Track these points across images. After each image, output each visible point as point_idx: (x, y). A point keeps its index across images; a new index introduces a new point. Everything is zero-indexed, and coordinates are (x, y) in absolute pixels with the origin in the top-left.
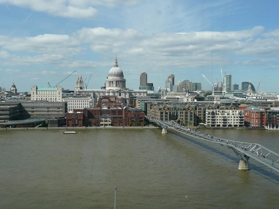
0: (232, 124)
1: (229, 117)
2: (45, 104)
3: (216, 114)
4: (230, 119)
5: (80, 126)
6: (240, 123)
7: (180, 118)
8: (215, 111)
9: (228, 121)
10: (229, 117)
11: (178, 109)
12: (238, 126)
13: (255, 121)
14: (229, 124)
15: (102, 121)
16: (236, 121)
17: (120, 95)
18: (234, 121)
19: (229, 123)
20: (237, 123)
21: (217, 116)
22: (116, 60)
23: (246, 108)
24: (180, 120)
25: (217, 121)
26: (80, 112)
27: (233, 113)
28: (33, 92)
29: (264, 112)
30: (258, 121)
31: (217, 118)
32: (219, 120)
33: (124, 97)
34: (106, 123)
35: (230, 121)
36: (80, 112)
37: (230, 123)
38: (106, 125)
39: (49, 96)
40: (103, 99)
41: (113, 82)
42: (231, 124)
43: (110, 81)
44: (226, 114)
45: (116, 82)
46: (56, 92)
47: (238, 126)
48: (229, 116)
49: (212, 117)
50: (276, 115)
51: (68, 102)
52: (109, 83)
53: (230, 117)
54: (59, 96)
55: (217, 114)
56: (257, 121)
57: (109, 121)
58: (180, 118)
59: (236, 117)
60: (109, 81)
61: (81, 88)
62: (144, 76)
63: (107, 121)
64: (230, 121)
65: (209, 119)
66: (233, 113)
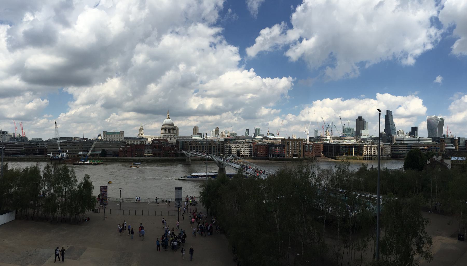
0: (244, 155)
3: (232, 147)
4: (243, 151)
6: (250, 154)
7: (206, 151)
8: (231, 145)
9: (241, 153)
11: (205, 144)
12: (249, 156)
14: (242, 155)
15: (146, 153)
16: (247, 153)
18: (245, 153)
19: (242, 154)
20: (248, 154)
21: (233, 148)
24: (205, 152)
25: (233, 153)
26: (129, 146)
29: (267, 146)
31: (233, 151)
32: (234, 152)
34: (148, 155)
36: (129, 146)
37: (243, 154)
38: (149, 156)
39: (118, 138)
40: (155, 140)
41: (165, 130)
45: (168, 130)
47: (249, 156)
48: (241, 148)
49: (229, 150)
50: (274, 147)
51: (128, 142)
53: (243, 149)
54: (122, 138)
57: (151, 153)
59: (247, 149)
63: (149, 153)
64: (243, 153)
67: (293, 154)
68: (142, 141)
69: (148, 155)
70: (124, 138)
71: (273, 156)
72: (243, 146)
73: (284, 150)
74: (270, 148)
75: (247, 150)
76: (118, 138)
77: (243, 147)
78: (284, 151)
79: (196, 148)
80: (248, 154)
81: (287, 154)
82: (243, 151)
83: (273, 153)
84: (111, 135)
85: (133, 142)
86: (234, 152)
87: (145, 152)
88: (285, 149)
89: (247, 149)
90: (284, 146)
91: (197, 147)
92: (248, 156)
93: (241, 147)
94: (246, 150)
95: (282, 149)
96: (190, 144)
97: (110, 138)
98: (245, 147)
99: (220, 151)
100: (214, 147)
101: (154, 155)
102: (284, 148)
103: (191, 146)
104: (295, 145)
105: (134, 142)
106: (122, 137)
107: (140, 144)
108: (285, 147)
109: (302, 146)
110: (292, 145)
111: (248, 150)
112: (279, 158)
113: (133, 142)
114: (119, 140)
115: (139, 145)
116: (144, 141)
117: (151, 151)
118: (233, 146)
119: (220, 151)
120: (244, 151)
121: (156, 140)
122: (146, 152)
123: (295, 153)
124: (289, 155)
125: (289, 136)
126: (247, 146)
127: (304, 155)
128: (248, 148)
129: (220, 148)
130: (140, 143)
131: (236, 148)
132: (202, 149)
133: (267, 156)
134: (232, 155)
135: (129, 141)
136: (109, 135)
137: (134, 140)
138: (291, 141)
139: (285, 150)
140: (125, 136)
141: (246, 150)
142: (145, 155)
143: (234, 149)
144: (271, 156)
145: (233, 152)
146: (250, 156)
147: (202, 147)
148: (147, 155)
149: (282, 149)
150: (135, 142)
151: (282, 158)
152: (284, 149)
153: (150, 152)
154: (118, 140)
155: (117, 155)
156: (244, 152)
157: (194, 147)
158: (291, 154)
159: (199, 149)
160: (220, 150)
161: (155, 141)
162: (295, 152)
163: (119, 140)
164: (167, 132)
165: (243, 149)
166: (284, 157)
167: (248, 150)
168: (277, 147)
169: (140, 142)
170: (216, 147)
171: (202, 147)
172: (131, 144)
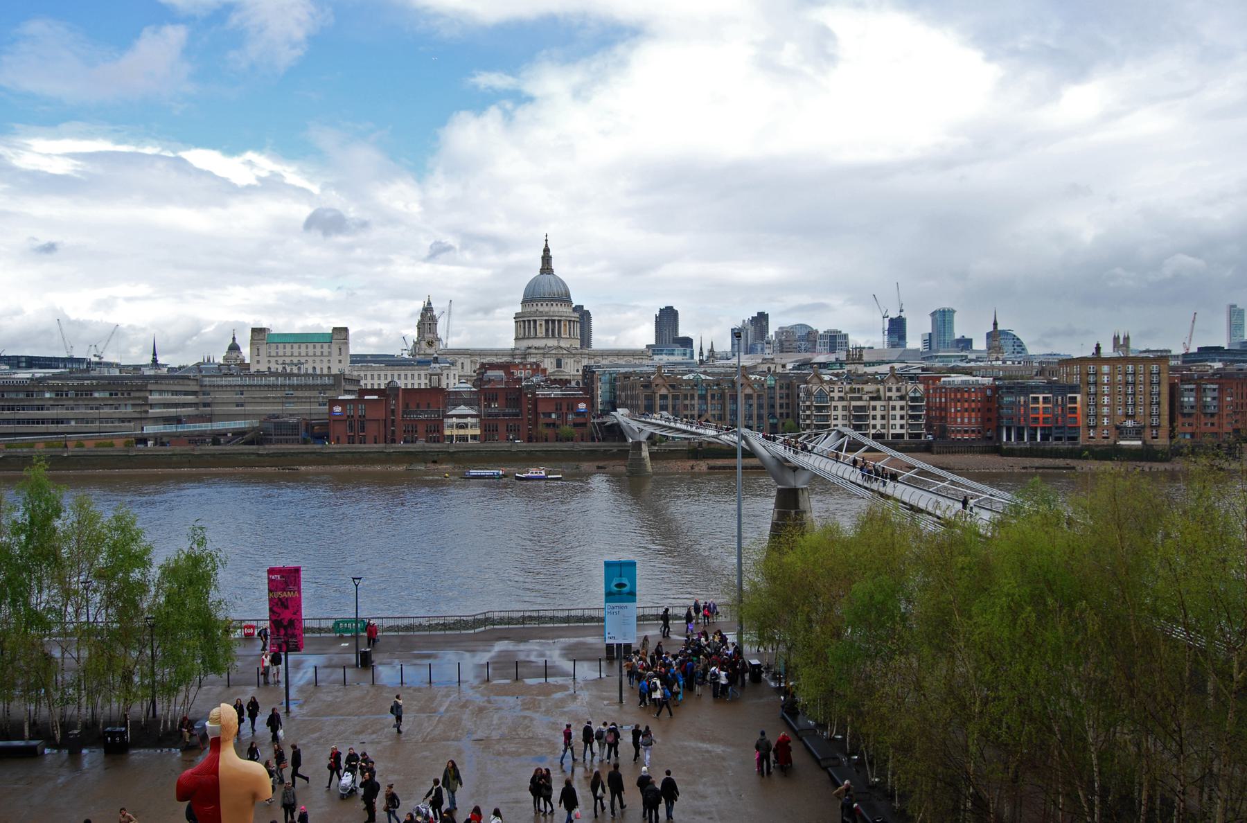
1: (874, 408)
2: (277, 379)
5: (375, 443)
8: (827, 388)
9: (873, 422)
10: (874, 408)
12: (906, 438)
13: (959, 420)
14: (873, 431)
15: (451, 426)
16: (898, 422)
17: (559, 365)
19: (874, 426)
21: (834, 404)
22: (547, 250)
23: (939, 381)
26: (376, 397)
27: (889, 394)
28: (258, 349)
30: (970, 419)
32: (840, 417)
33: (572, 373)
34: (462, 432)
35: (878, 422)
36: (376, 397)
38: (463, 438)
40: (489, 369)
41: (535, 321)
42: (882, 431)
43: (525, 319)
44: (866, 397)
45: (547, 321)
46: (329, 347)
47: (906, 438)
48: (873, 403)
49: (819, 409)
51: (369, 377)
52: (524, 328)
54: (340, 361)
55: (836, 398)
56: (966, 420)
58: (714, 416)
59: (898, 408)
60: (524, 321)
61: (430, 344)
62: (667, 318)
65: (808, 417)
66: (889, 394)
67: (1117, 428)
68: (431, 375)
69: (462, 432)
70: (352, 362)
71: (1020, 437)
72: (878, 391)
73: (1075, 408)
74: (1007, 399)
75: (898, 413)
76: (325, 359)
77: (878, 398)
78: (1074, 413)
79: (670, 402)
80: (902, 427)
81: (1089, 427)
82: (878, 413)
83: (1022, 423)
84: (288, 346)
85: (393, 375)
86: (840, 417)
87: (445, 420)
88: (1078, 405)
89: (899, 404)
90: (1074, 389)
91: (675, 398)
92: (901, 436)
93: (872, 399)
94: (894, 408)
95: (1064, 404)
96: (647, 386)
97: (288, 360)
98: (890, 398)
99: (778, 416)
100: (748, 397)
101: (489, 430)
102: (1075, 398)
103: (648, 392)
104: (1127, 383)
105: (396, 379)
106: (340, 358)
107: (423, 387)
108: (1079, 397)
109: (1165, 390)
110: (1111, 384)
111: (902, 408)
112: (1052, 443)
113: (393, 375)
114: (329, 368)
115: (419, 390)
116: (439, 371)
117: (472, 416)
118: (836, 395)
119: (778, 416)
120: (883, 413)
121: (493, 366)
122: (450, 421)
123: (1129, 423)
124: (1099, 430)
125: (1098, 345)
126: (898, 394)
127: (1172, 437)
128: (903, 403)
129: (778, 401)
130: (423, 383)
131: (845, 403)
132: (696, 409)
133: (990, 438)
134: (839, 432)
135: (372, 375)
136: (281, 346)
137: (396, 368)
138: (1106, 369)
139: (1079, 411)
140: (352, 352)
141: (894, 408)
142: (447, 432)
143: (840, 404)
144: (1009, 438)
145: (837, 419)
146: (911, 436)
147: (696, 398)
148: (455, 432)
149: (1064, 404)
150: (403, 377)
151: (1064, 445)
152: (1076, 403)
153: (469, 419)
154: (322, 369)
155: (322, 437)
156: (883, 417)
157: (664, 397)
158: (1107, 428)
159: (686, 407)
160: (778, 411)
161: (490, 373)
162: (1127, 416)
163: (329, 368)
164: (541, 331)
165: (878, 404)
166: (1075, 439)
167: (902, 408)
168: (1041, 397)
169: (423, 377)
170: (759, 397)
171: (696, 398)
172: (383, 387)
